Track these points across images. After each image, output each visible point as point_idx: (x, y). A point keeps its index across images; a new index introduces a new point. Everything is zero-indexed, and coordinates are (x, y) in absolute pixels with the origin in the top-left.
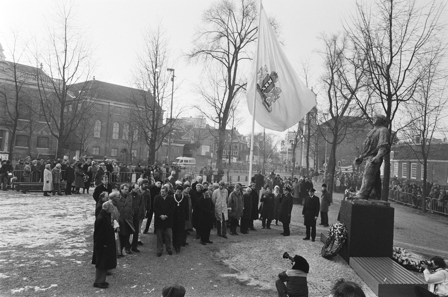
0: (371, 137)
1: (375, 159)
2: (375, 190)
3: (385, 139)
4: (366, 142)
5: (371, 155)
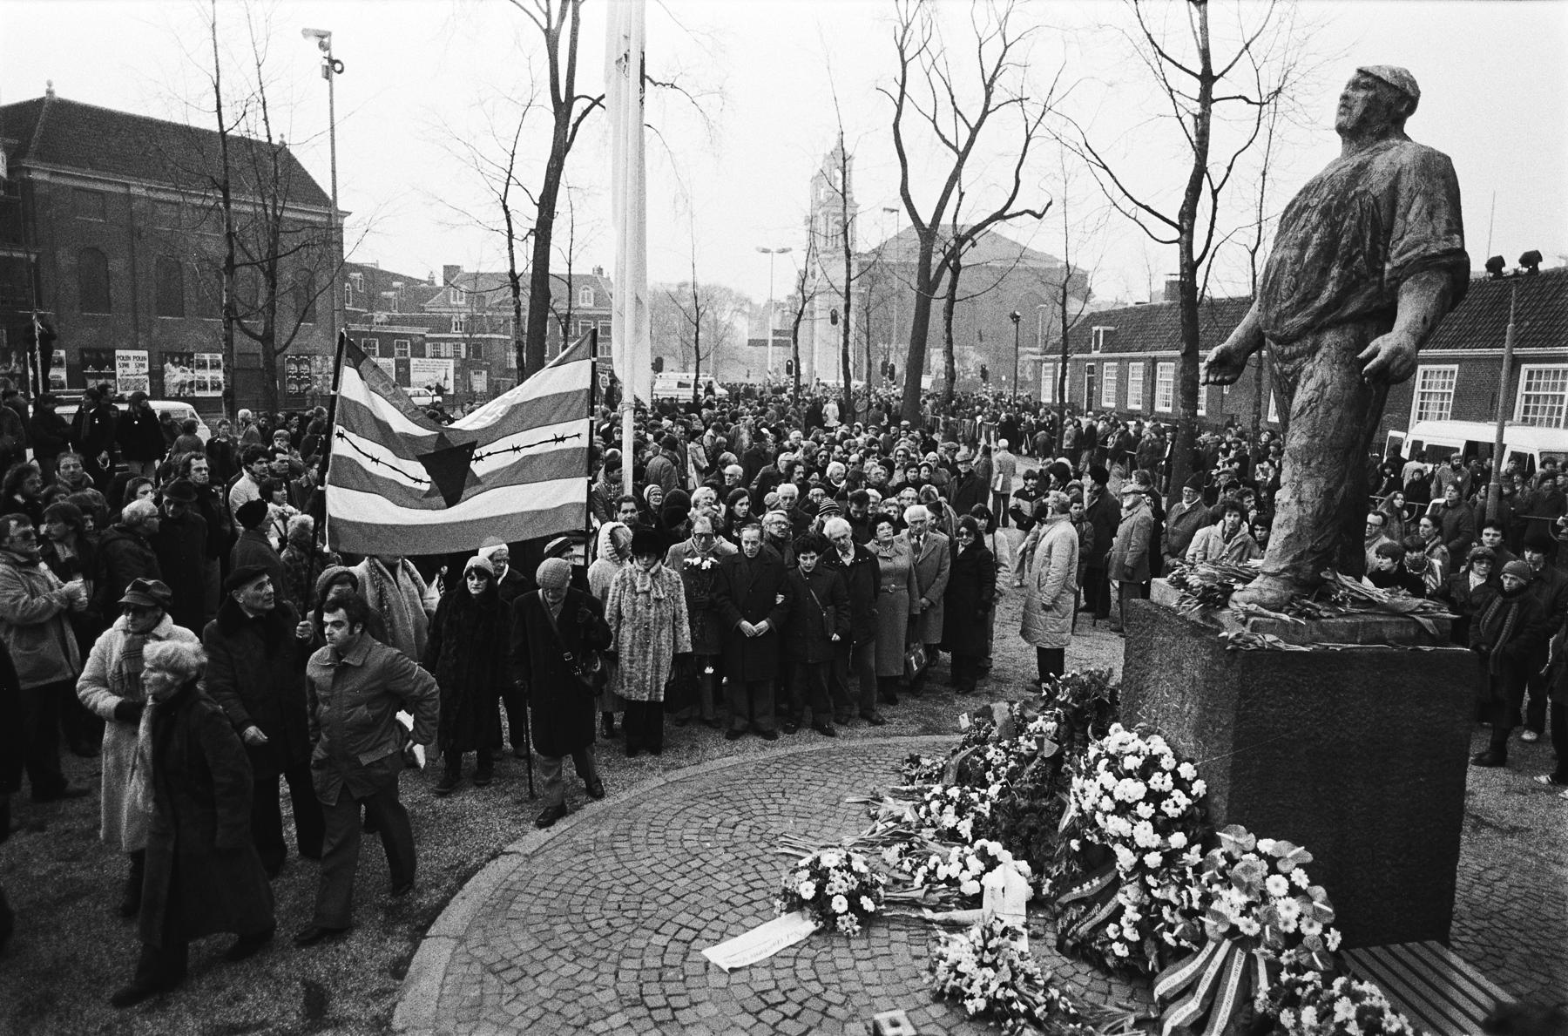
1: (1397, 352)
4: (1303, 245)
5: (1338, 324)
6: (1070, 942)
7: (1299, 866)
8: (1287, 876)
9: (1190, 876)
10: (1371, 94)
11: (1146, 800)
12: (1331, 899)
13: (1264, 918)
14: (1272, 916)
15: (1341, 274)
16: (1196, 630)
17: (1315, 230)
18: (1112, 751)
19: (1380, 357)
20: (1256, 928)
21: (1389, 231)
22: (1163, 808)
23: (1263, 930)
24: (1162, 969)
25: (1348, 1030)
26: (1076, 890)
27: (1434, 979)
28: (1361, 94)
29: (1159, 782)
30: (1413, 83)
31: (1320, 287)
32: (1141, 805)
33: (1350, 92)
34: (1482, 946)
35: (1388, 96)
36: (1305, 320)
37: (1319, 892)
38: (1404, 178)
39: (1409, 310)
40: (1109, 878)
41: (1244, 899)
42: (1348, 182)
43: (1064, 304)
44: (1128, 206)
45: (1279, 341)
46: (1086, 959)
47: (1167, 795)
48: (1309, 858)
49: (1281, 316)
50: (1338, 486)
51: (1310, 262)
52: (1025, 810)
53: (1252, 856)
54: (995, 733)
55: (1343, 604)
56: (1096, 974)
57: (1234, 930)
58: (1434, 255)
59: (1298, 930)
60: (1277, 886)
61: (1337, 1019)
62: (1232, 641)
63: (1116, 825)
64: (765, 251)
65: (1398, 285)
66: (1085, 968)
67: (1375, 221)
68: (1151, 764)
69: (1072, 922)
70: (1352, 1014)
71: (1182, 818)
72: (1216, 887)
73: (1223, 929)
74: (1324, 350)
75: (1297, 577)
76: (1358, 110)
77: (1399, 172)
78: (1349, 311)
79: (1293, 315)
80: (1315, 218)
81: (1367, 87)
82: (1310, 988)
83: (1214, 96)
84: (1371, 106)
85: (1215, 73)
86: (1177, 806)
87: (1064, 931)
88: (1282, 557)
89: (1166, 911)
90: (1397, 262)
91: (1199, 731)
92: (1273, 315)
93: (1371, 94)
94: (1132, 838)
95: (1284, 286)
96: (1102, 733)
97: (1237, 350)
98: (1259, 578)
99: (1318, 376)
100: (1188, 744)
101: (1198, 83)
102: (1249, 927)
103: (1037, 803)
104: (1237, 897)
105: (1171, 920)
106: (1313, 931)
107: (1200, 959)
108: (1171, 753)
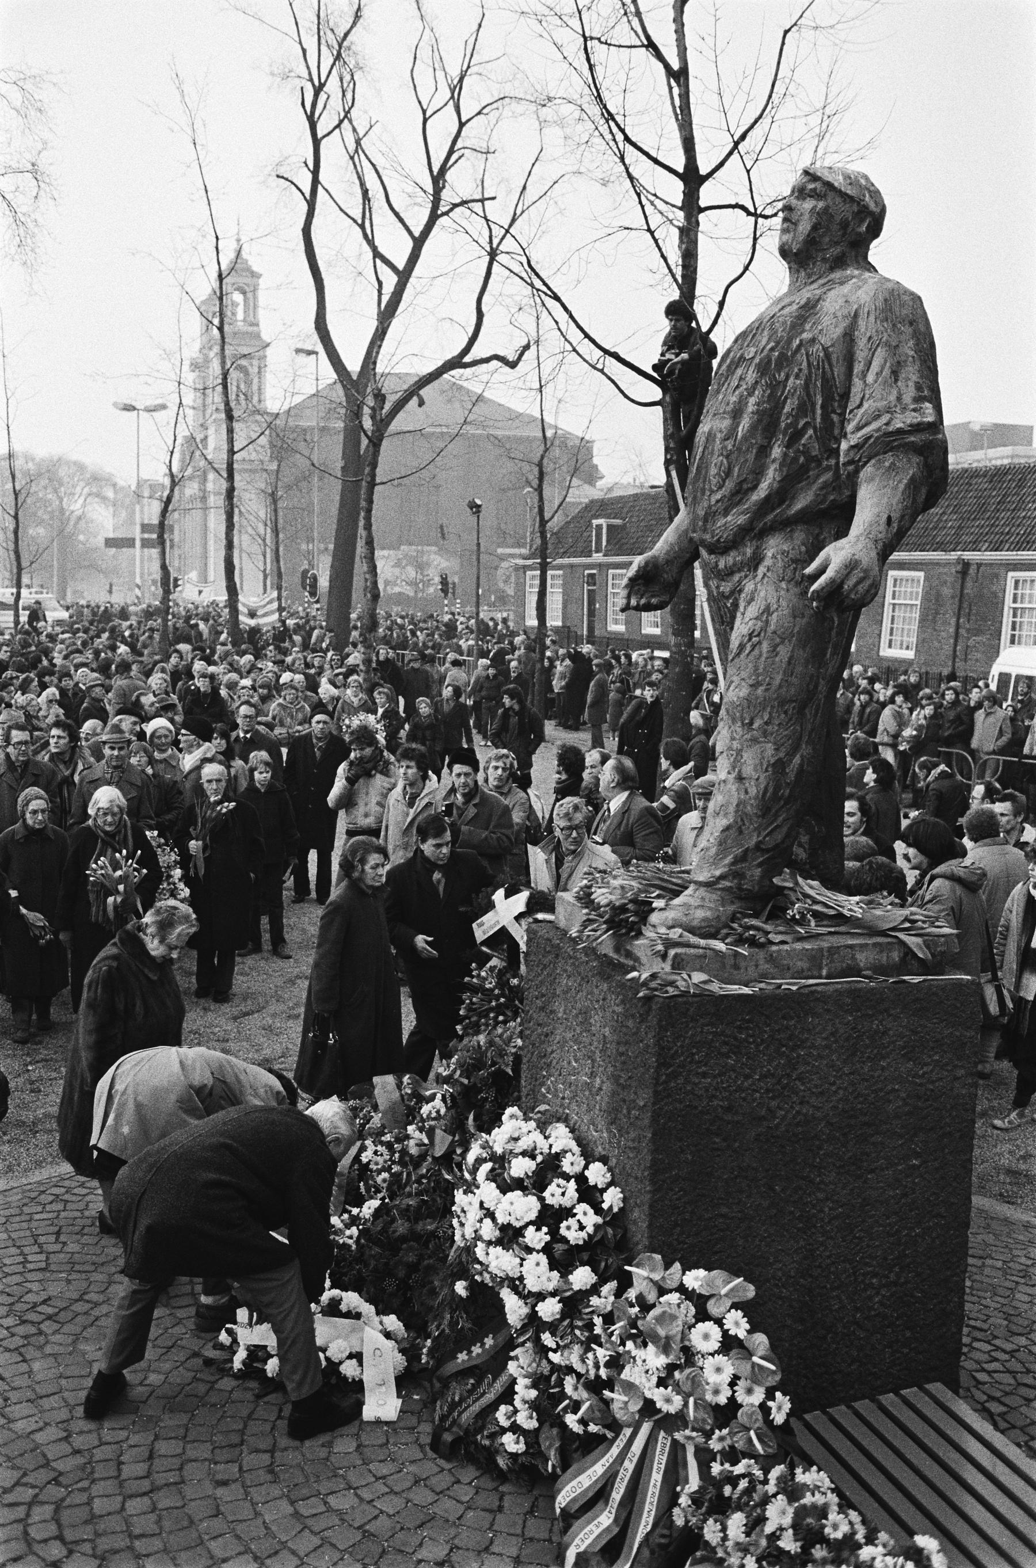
0: (784, 360)
1: (851, 566)
4: (737, 414)
5: (784, 525)
6: (448, 1437)
7: (735, 1306)
8: (719, 1322)
9: (598, 1330)
10: (821, 204)
11: (538, 1223)
12: (776, 1352)
13: (687, 1388)
14: (696, 1382)
15: (785, 455)
16: (609, 970)
17: (751, 394)
18: (499, 1150)
19: (830, 573)
20: (678, 1400)
21: (846, 396)
22: (563, 1231)
23: (686, 1405)
24: (564, 1469)
25: (781, 1544)
26: (462, 1357)
27: (931, 1439)
28: (808, 205)
29: (560, 1193)
30: (876, 194)
31: (758, 473)
32: (531, 1228)
33: (794, 202)
34: (1013, 1373)
35: (846, 211)
36: (742, 520)
37: (761, 1340)
38: (862, 323)
39: (873, 503)
40: (501, 1338)
41: (662, 1361)
42: (793, 326)
43: (540, 490)
44: (586, 348)
45: (712, 550)
46: (471, 1459)
47: (567, 1213)
48: (751, 1292)
49: (710, 516)
50: (791, 754)
51: (745, 438)
52: (403, 1239)
53: (674, 1298)
54: (377, 1120)
55: (802, 922)
56: (487, 1483)
57: (649, 1408)
58: (900, 432)
59: (732, 1399)
60: (705, 1337)
61: (769, 1528)
62: (645, 984)
63: (500, 1261)
64: (129, 408)
65: (857, 471)
66: (469, 1474)
67: (827, 383)
68: (550, 1167)
69: (453, 1406)
70: (787, 1520)
71: (590, 1244)
72: (630, 1345)
73: (635, 1406)
74: (768, 562)
75: (739, 888)
76: (804, 227)
77: (856, 315)
78: (799, 505)
79: (726, 512)
80: (751, 376)
81: (814, 195)
82: (743, 1484)
83: (703, 203)
84: (822, 221)
85: (703, 171)
86: (582, 1228)
87: (443, 1418)
88: (715, 862)
89: (569, 1382)
90: (854, 439)
91: (613, 1115)
92: (701, 513)
93: (821, 204)
94: (521, 1278)
95: (713, 471)
96: (490, 1122)
97: (668, 562)
98: (689, 891)
99: (764, 597)
100: (599, 1136)
101: (679, 185)
102: (668, 1401)
103: (419, 1227)
104: (654, 1359)
105: (575, 1397)
106: (751, 1399)
107: (615, 1451)
108: (576, 1149)
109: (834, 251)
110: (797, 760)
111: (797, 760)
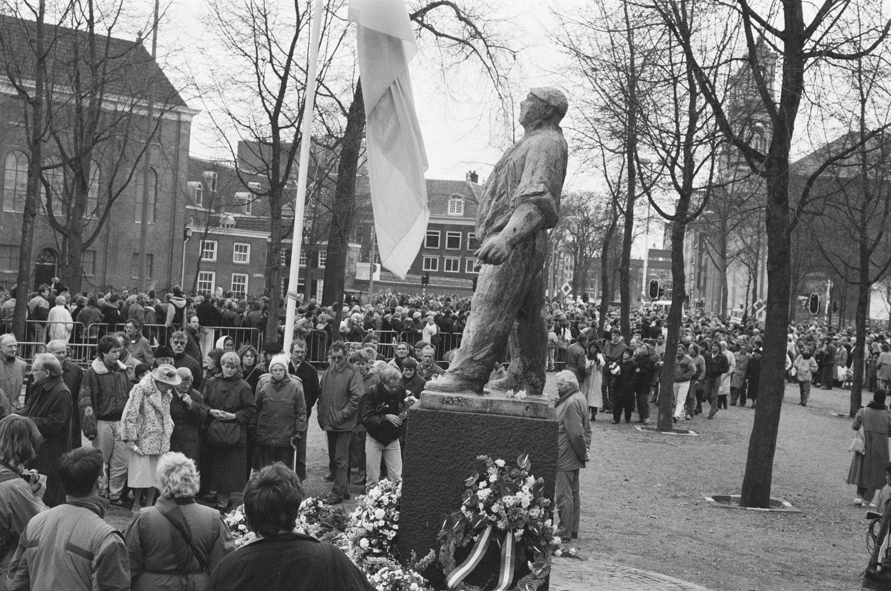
1: (491, 247)
2: (523, 361)
3: (539, 173)
58: (527, 196)
109: (538, 121)
110: (492, 325)
111: (492, 325)
